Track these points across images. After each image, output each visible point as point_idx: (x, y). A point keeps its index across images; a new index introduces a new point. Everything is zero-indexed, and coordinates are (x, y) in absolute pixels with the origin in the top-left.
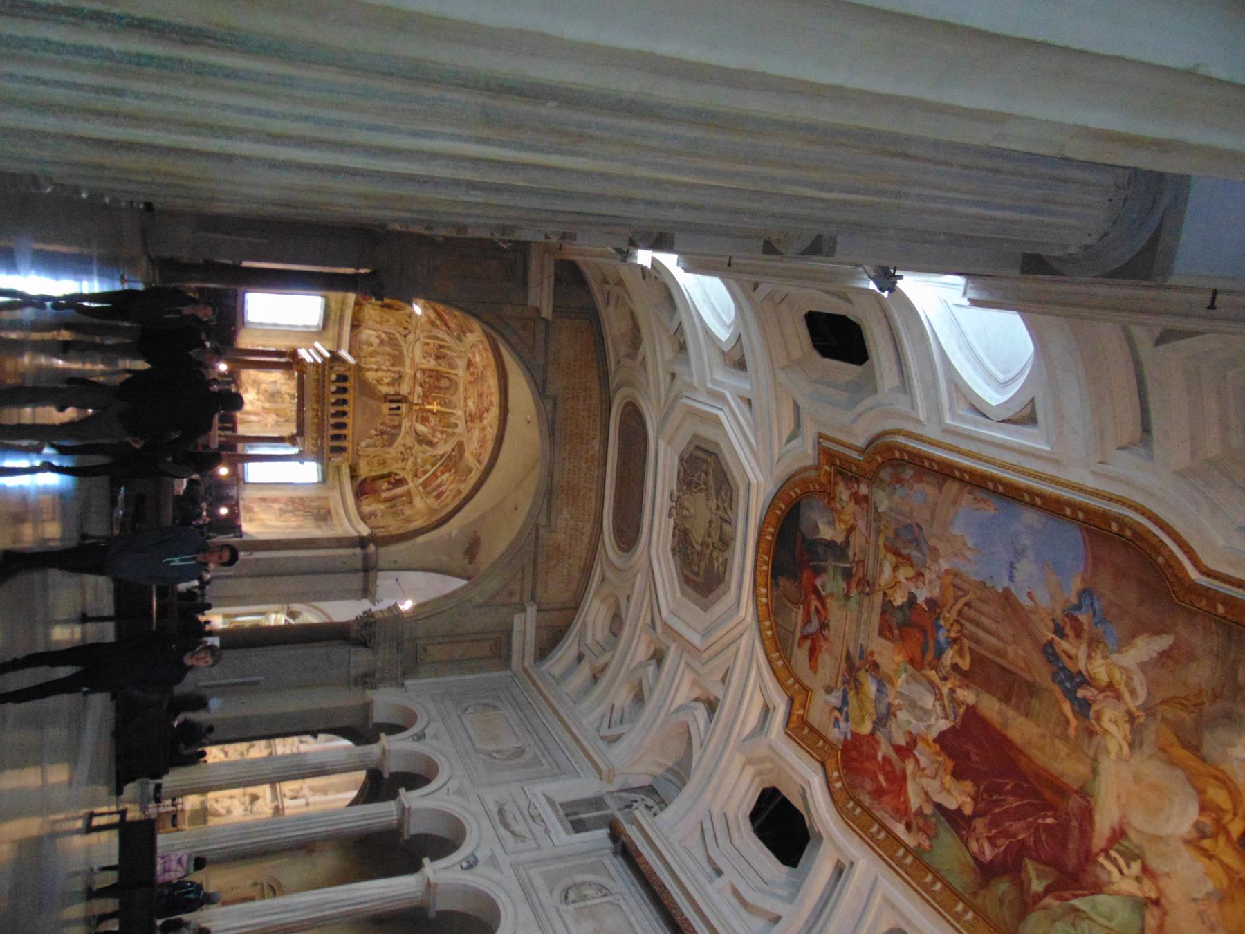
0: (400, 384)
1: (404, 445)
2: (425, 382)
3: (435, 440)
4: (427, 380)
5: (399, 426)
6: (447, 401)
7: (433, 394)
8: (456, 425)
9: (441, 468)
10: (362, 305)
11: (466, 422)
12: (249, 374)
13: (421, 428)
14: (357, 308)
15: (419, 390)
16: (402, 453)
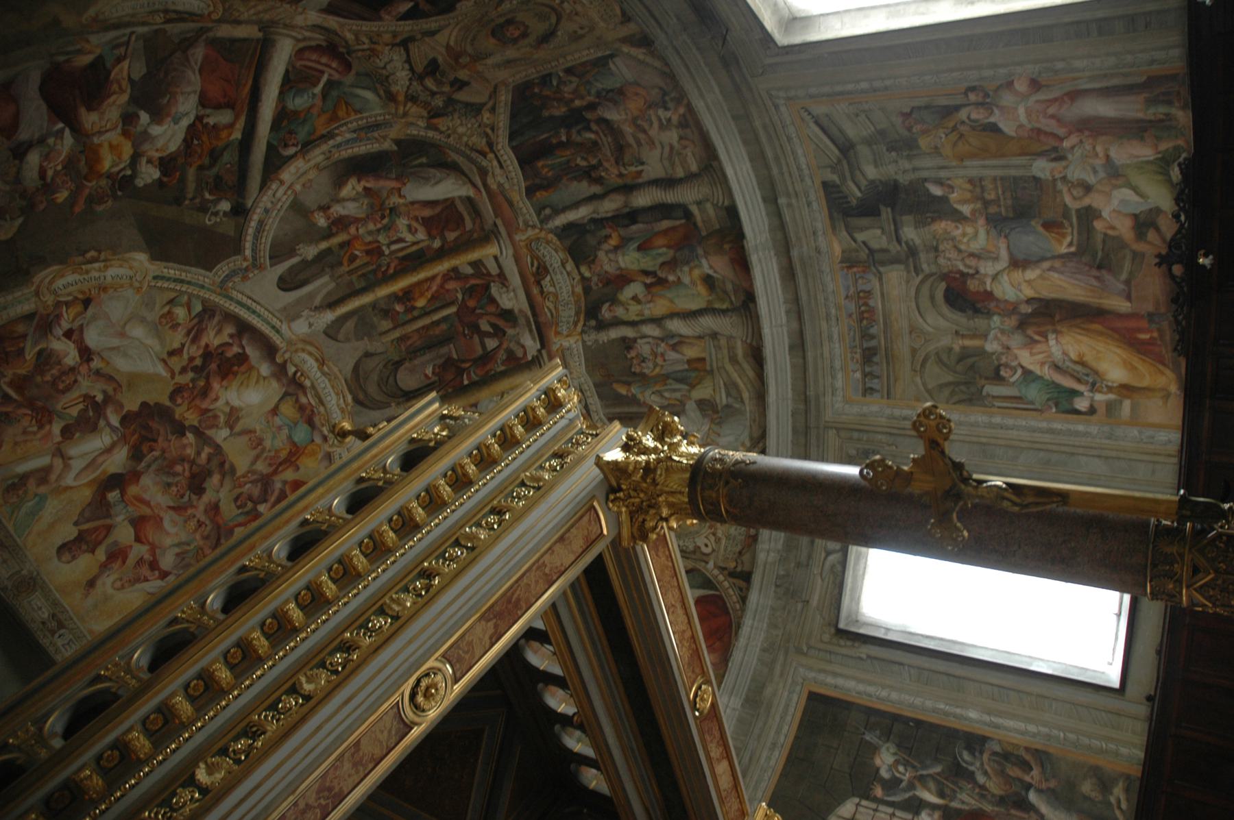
0: (587, 290)
1: (474, 109)
2: (498, 332)
3: (352, 187)
4: (491, 344)
5: (526, 160)
6: (386, 325)
7: (453, 309)
8: (286, 284)
9: (237, 135)
10: (732, 574)
11: (244, 329)
12: (1129, 298)
13: (447, 188)
14: (746, 568)
15: (511, 299)
16: (460, 85)
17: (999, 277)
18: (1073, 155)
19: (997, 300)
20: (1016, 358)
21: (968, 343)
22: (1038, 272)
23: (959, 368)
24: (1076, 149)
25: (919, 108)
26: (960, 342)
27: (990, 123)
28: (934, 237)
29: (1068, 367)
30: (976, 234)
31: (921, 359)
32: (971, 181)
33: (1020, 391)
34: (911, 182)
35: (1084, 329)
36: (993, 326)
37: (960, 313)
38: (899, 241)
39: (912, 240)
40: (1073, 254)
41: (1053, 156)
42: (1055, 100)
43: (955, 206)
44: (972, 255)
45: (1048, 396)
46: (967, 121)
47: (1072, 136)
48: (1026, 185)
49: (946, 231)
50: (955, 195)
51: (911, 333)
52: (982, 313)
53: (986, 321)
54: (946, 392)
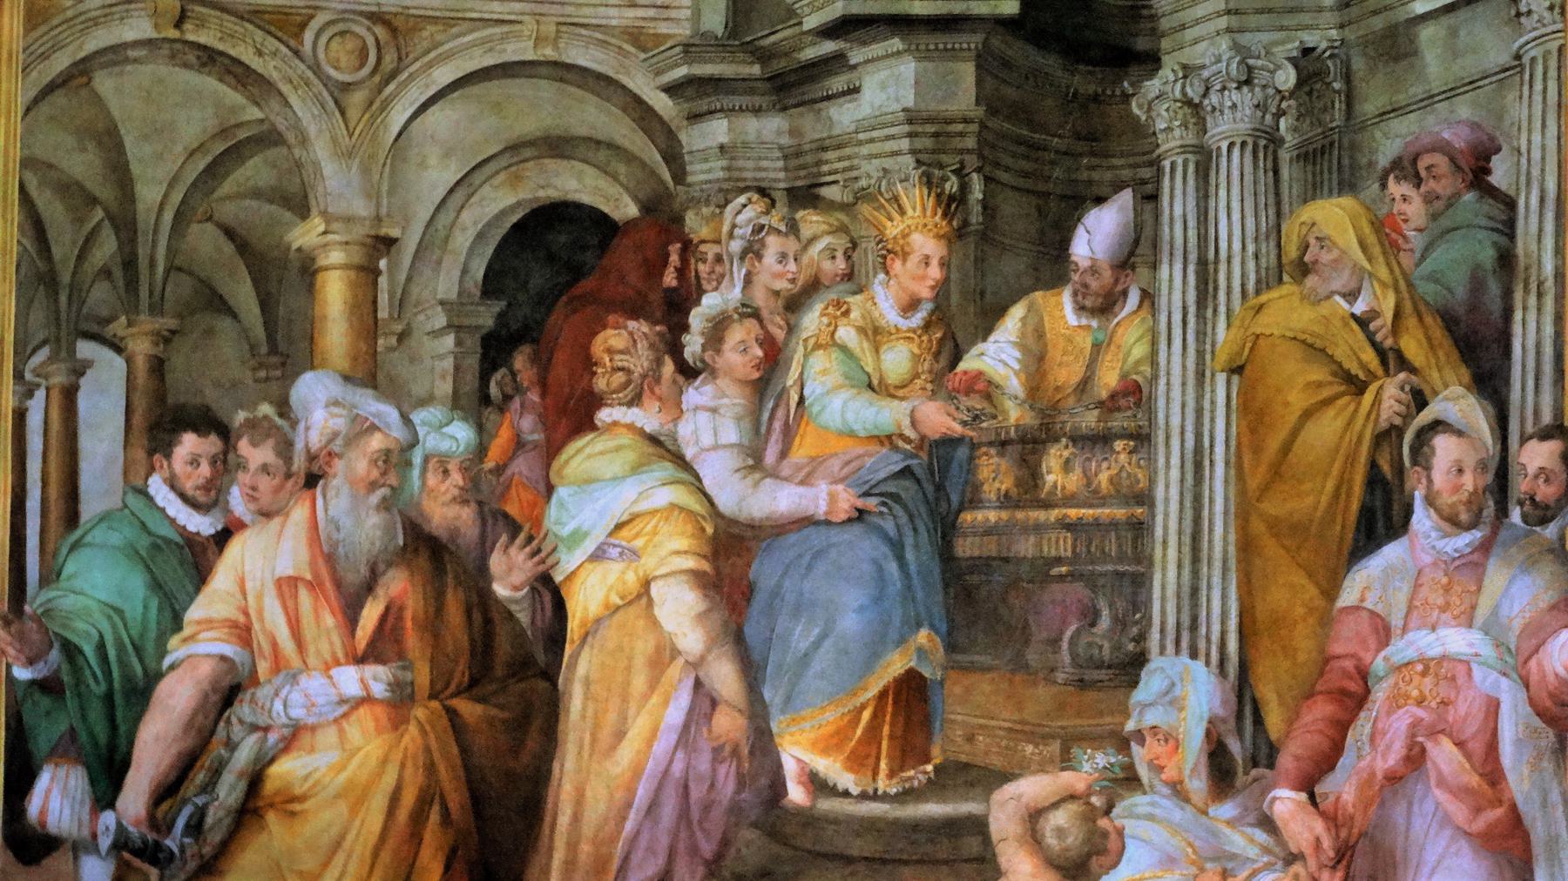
17: (667, 469)
18: (1229, 823)
19: (551, 450)
20: (267, 514)
21: (334, 292)
22: (691, 639)
23: (204, 241)
24: (1261, 836)
25: (1508, 228)
26: (336, 257)
27: (1408, 511)
28: (862, 196)
29: (231, 746)
30: (876, 387)
31: (245, 54)
32: (1134, 394)
33: (104, 517)
34: (1141, 132)
35: (418, 817)
36: (418, 417)
37: (479, 270)
38: (845, 27)
39: (854, 91)
40: (777, 787)
41: (1234, 746)
42: (1493, 773)
43: (1017, 312)
44: (773, 357)
45: (89, 650)
46: (1425, 417)
47: (1319, 826)
48: (1105, 622)
49: (889, 254)
50: (1072, 318)
51: (376, 18)
52: (484, 379)
53: (445, 387)
54: (83, 165)
